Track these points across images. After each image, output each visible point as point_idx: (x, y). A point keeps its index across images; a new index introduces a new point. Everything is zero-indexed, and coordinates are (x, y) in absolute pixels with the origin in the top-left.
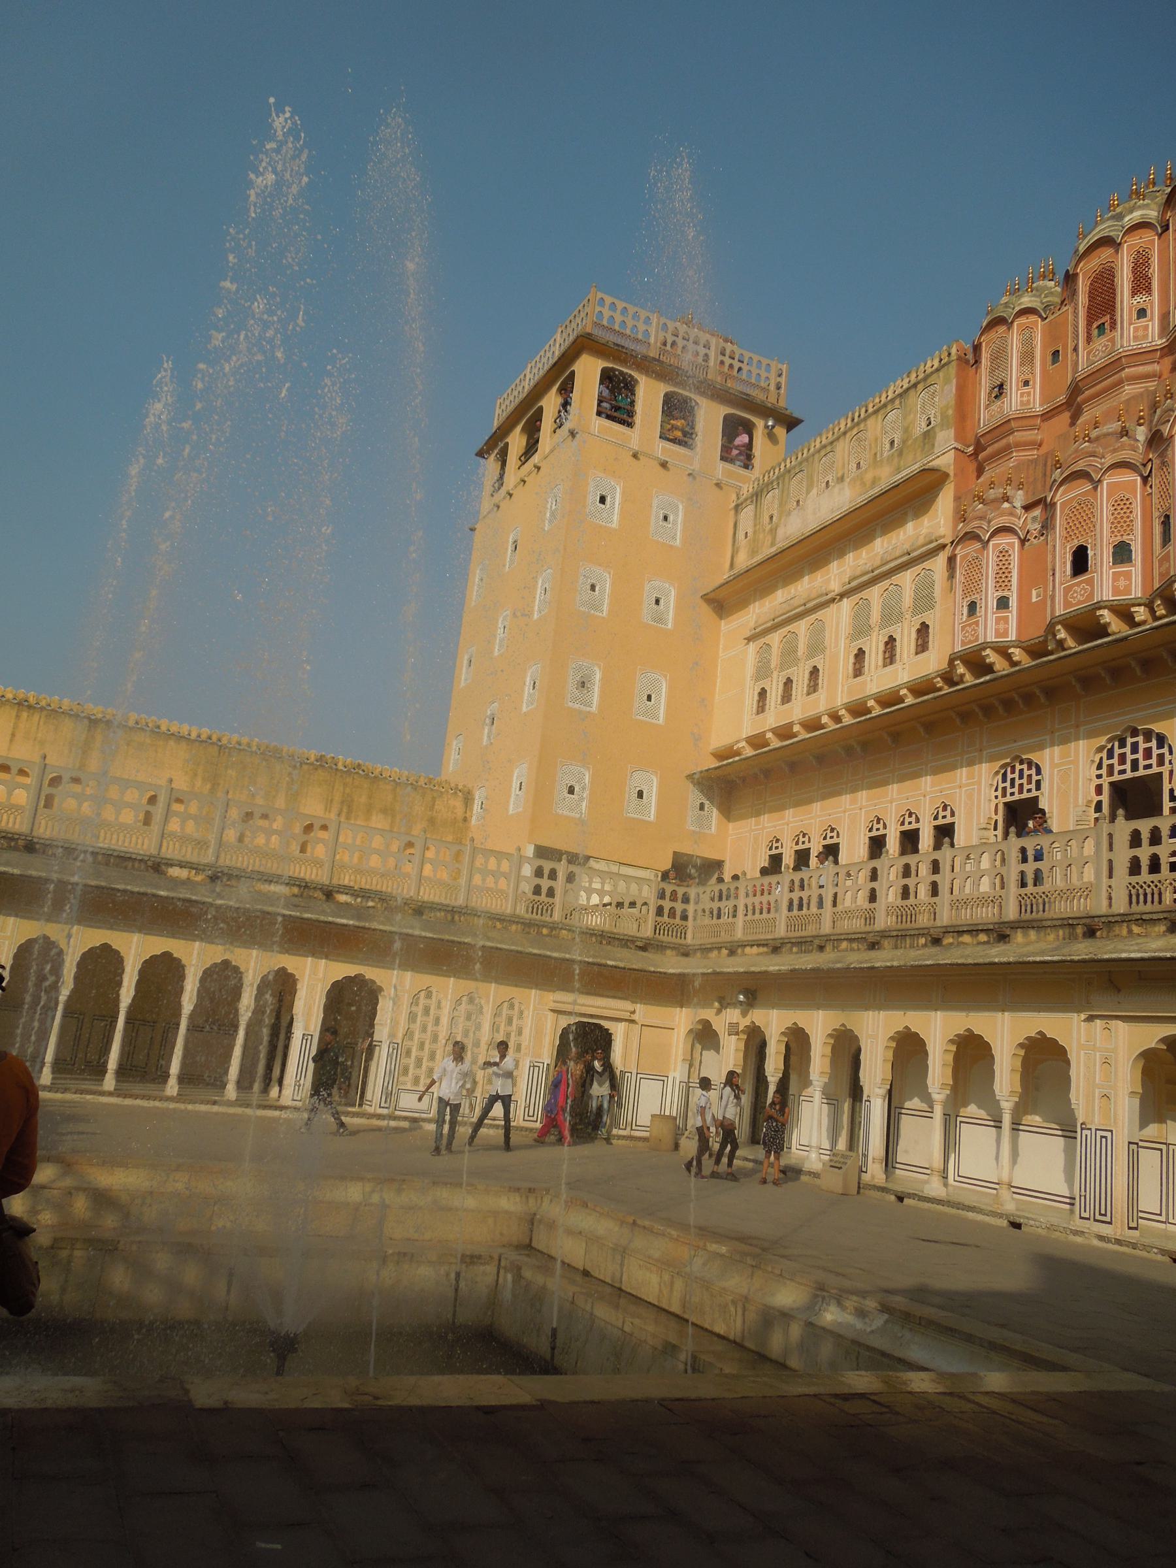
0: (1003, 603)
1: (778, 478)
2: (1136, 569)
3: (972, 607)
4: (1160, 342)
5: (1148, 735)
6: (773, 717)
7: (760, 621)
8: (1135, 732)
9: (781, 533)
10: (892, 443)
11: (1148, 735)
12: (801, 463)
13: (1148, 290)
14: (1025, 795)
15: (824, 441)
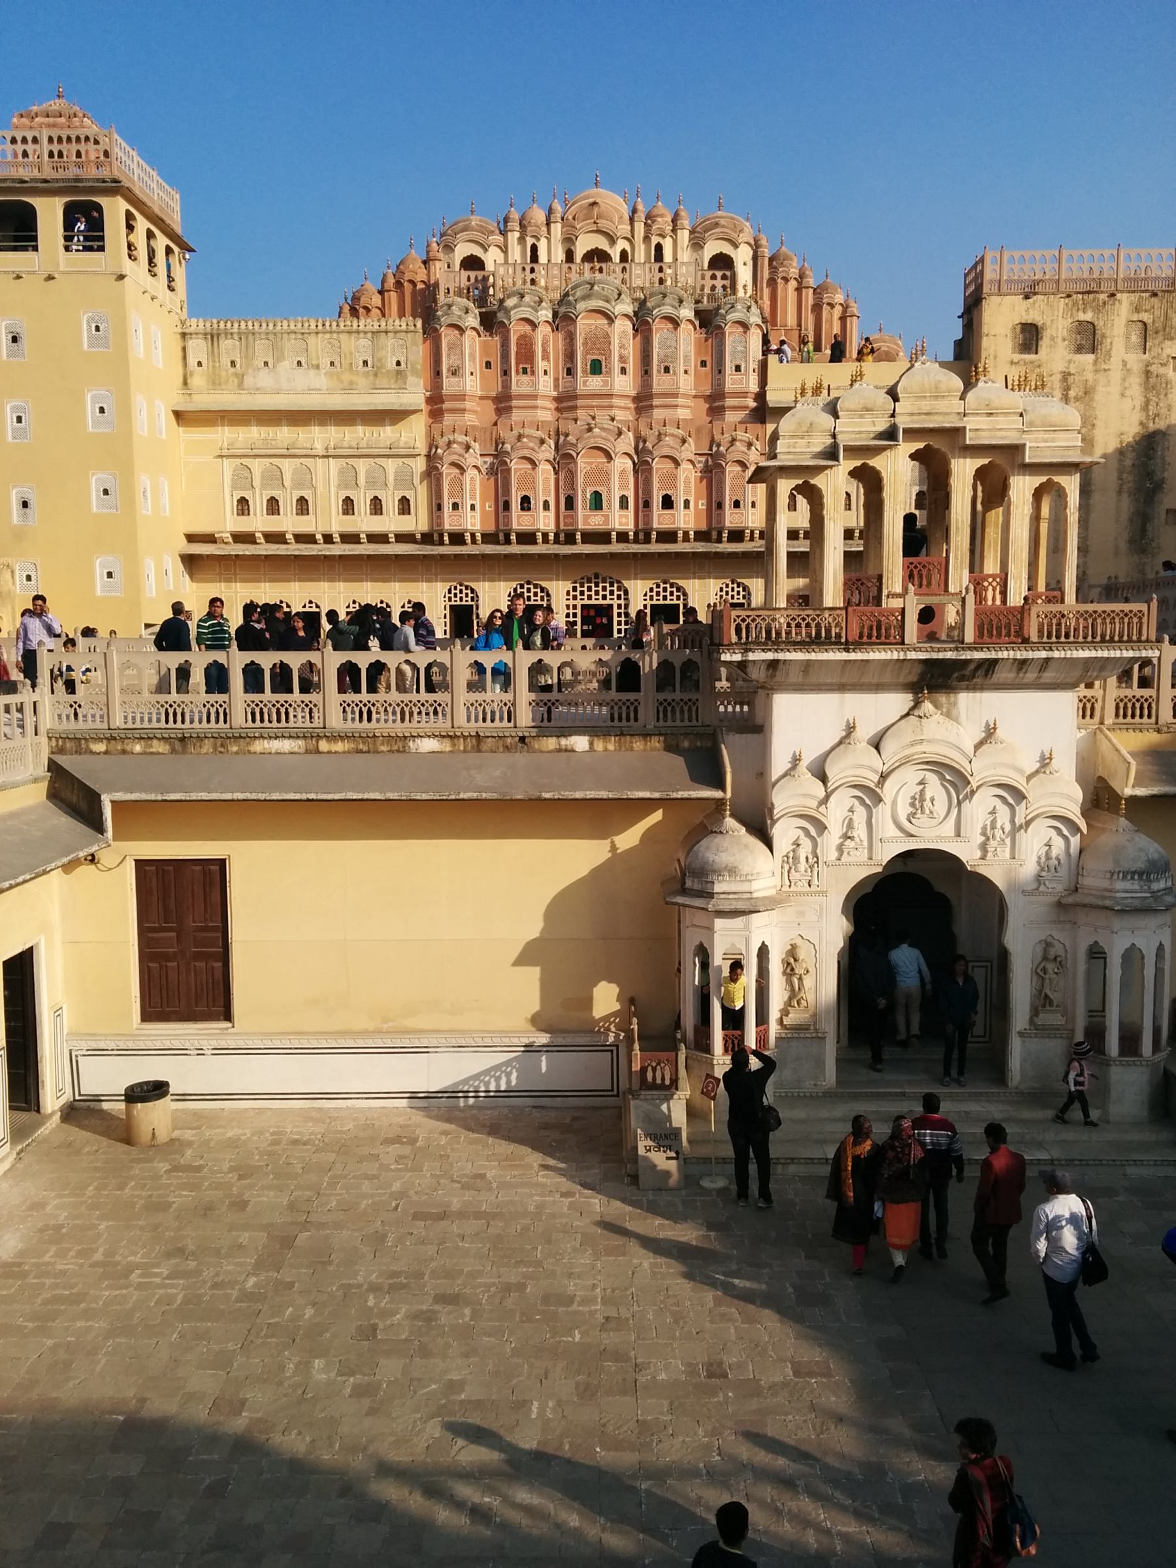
0: (473, 507)
1: (239, 333)
2: (552, 514)
3: (455, 506)
4: (555, 394)
5: (536, 586)
6: (258, 522)
7: (237, 446)
8: (529, 583)
9: (249, 381)
10: (365, 363)
11: (536, 586)
12: (267, 334)
13: (549, 361)
14: (464, 603)
15: (292, 327)
